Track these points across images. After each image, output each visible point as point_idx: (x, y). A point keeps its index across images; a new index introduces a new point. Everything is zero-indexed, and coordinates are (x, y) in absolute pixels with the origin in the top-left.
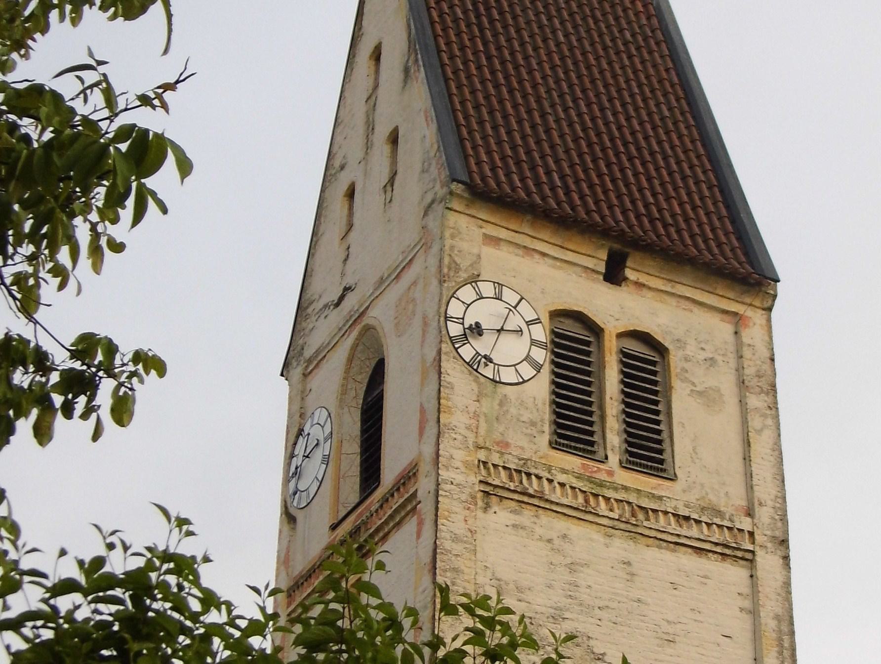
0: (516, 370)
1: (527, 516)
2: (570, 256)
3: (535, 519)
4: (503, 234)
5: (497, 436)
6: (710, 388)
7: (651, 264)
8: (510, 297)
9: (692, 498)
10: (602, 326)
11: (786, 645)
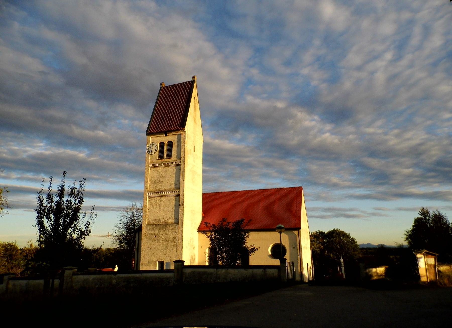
2: (161, 135)
5: (152, 161)
8: (154, 144)
9: (174, 160)
11: (183, 174)
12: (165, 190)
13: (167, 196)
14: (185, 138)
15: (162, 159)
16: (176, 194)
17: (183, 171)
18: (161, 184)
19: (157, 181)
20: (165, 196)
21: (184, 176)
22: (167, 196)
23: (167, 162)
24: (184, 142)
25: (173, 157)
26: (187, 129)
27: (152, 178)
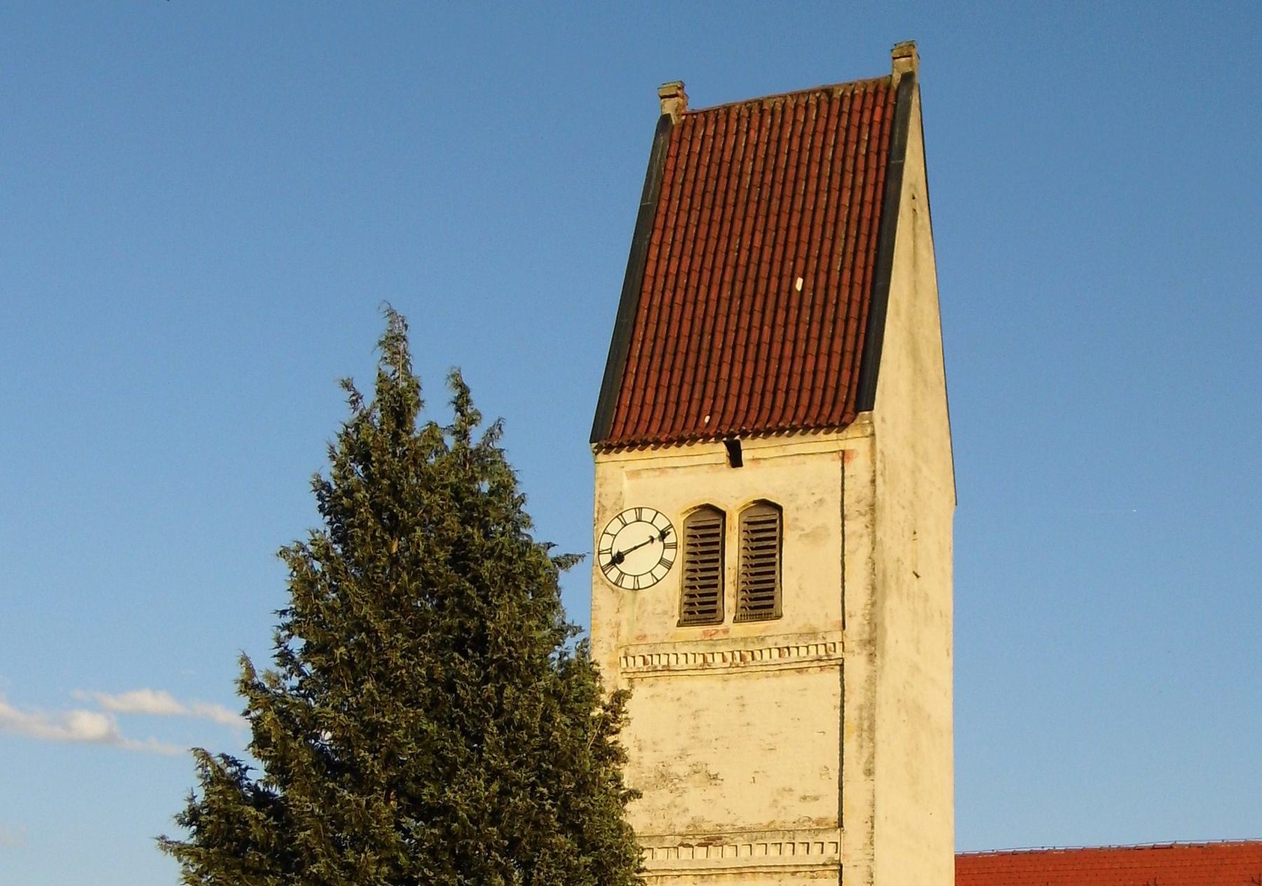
0: (652, 574)
1: (662, 685)
2: (696, 460)
3: (668, 686)
4: (642, 465)
5: (637, 633)
6: (818, 527)
7: (759, 441)
8: (647, 515)
9: (794, 629)
10: (724, 509)
12: (742, 831)
13: (754, 871)
14: (873, 481)
15: (707, 622)
16: (815, 856)
17: (861, 708)
18: (712, 792)
19: (680, 769)
20: (740, 872)
21: (872, 740)
22: (754, 871)
23: (744, 640)
24: (863, 507)
25: (786, 611)
26: (883, 420)
27: (640, 750)
